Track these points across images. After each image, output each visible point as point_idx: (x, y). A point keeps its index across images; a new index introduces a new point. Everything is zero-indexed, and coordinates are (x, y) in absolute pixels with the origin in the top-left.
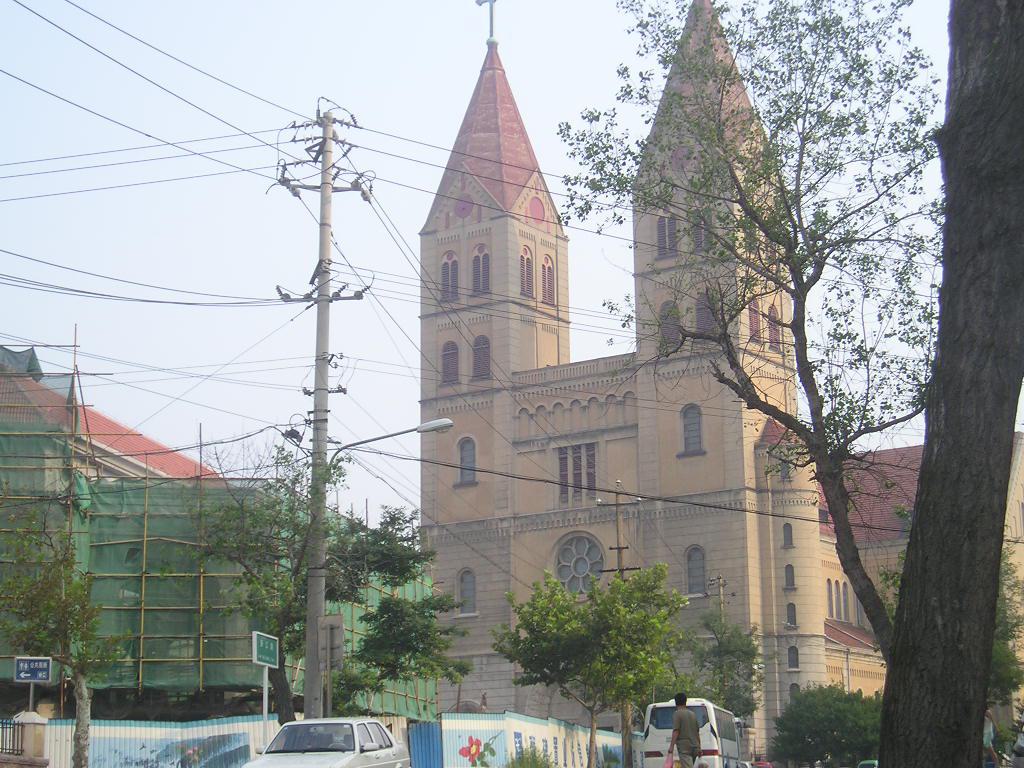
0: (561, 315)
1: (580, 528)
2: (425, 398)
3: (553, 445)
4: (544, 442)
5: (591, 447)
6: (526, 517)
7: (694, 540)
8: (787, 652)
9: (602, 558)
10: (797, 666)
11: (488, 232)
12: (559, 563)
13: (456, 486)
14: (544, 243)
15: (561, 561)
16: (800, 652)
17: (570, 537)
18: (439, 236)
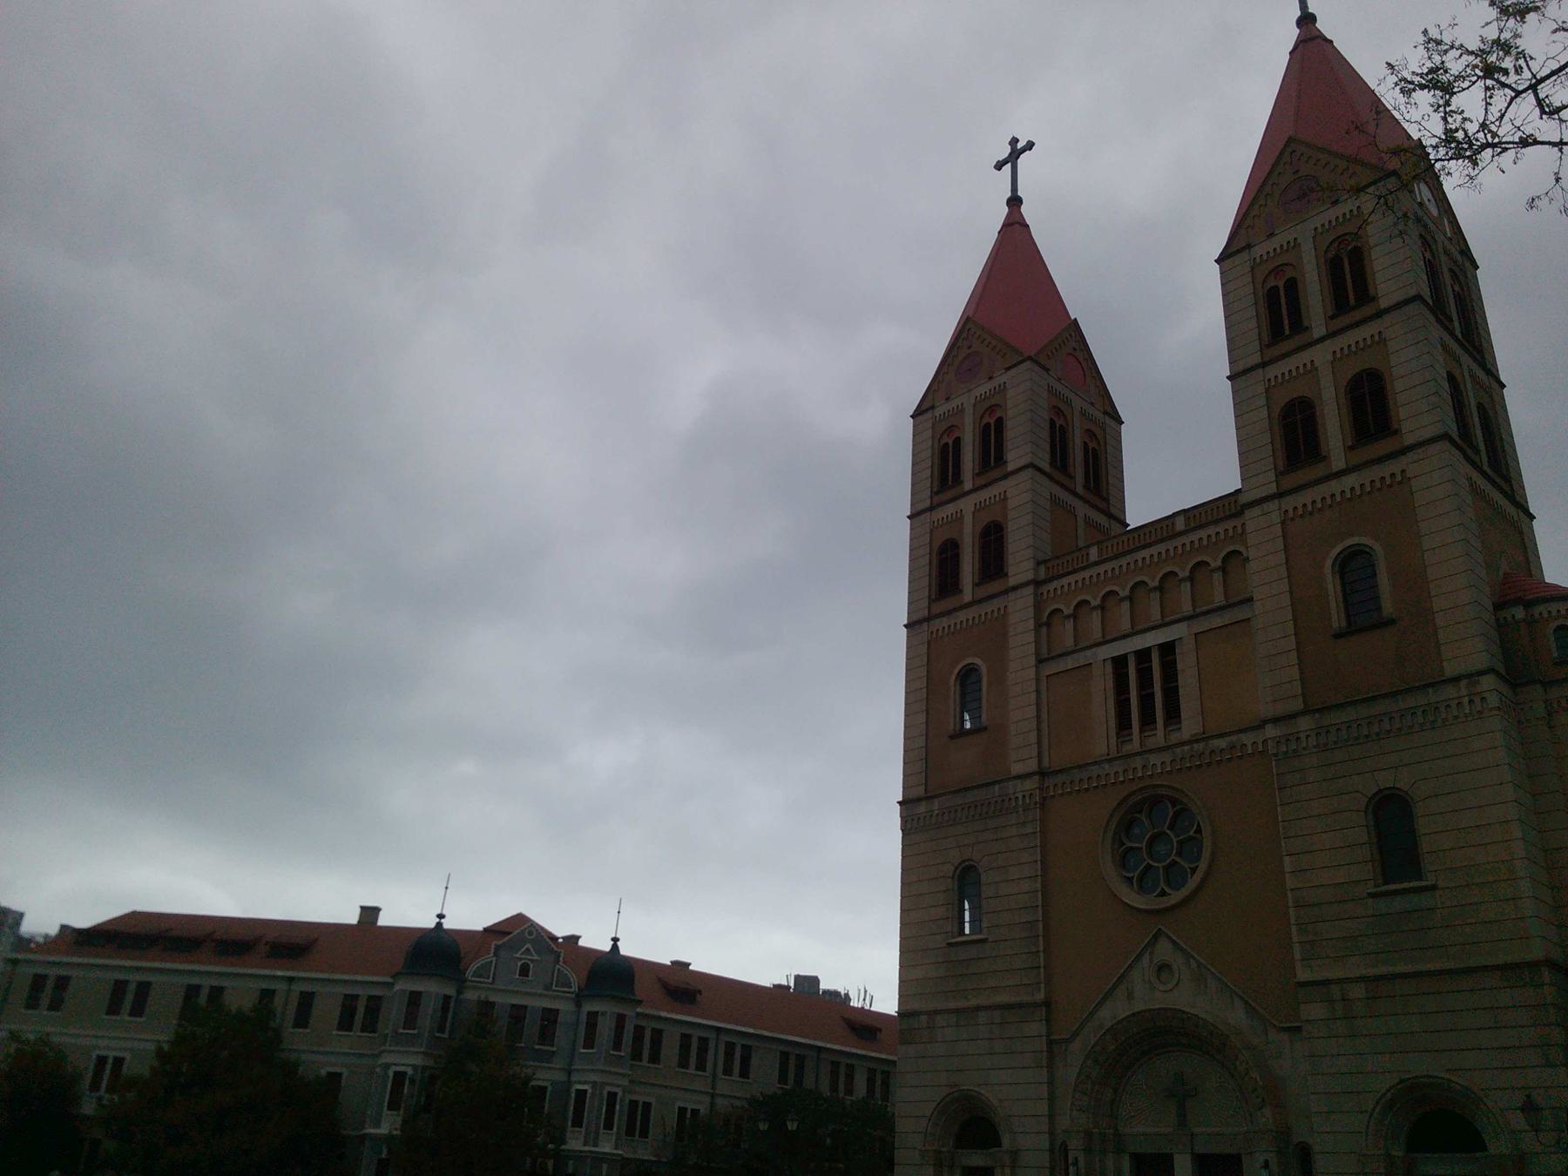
0: (1113, 510)
2: (915, 618)
7: (1385, 780)
11: (1002, 389)
13: (952, 737)
14: (1083, 413)
18: (938, 412)
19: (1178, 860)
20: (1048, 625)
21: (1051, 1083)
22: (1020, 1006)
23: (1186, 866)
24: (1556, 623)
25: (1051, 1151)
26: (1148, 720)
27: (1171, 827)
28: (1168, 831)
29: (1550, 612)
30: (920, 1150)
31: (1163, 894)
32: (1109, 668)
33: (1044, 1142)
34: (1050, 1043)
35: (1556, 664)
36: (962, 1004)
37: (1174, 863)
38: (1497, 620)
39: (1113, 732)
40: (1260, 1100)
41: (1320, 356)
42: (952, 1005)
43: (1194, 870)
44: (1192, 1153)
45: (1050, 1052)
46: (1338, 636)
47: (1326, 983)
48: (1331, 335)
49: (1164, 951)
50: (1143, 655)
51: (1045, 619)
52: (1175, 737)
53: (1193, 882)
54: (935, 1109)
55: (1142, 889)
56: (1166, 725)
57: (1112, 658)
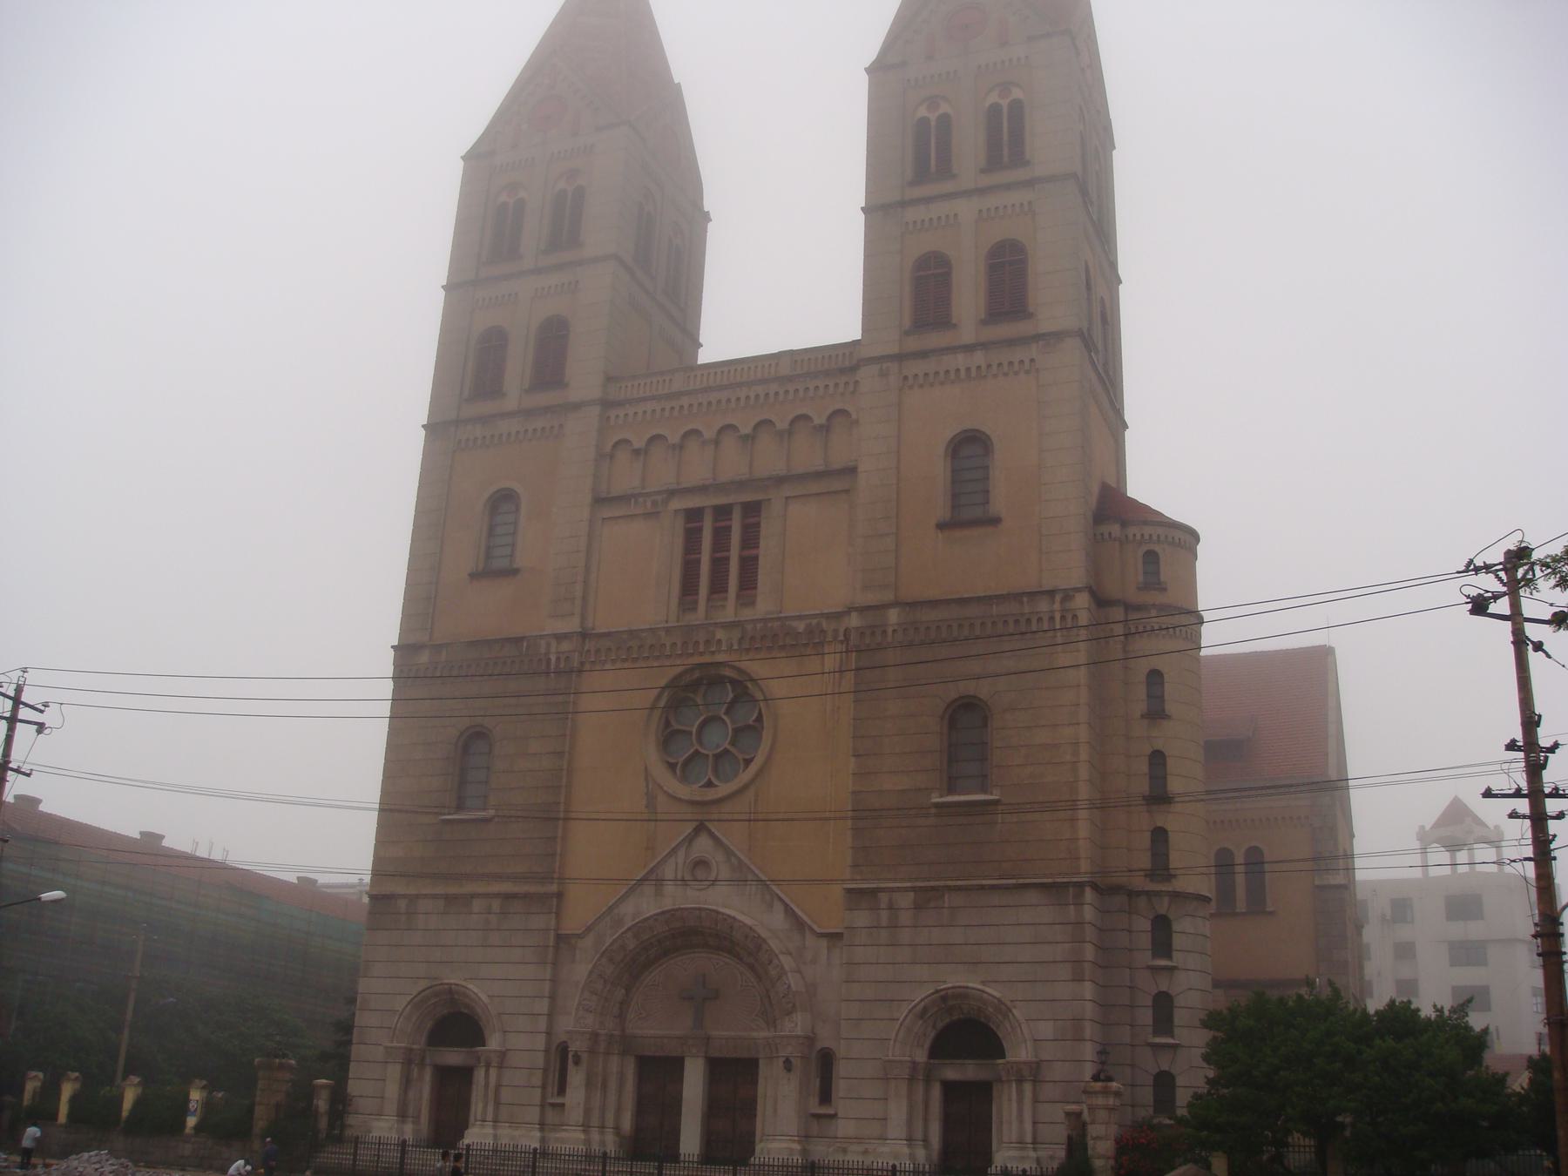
1: (720, 658)
3: (678, 504)
4: (659, 498)
5: (752, 510)
6: (608, 634)
7: (968, 688)
8: (1147, 925)
9: (759, 719)
10: (1170, 957)
12: (668, 723)
15: (673, 722)
16: (1176, 927)
17: (697, 674)
19: (732, 749)
20: (612, 457)
21: (554, 981)
22: (526, 896)
23: (740, 757)
24: (1145, 548)
25: (547, 1051)
26: (718, 587)
27: (727, 713)
28: (725, 717)
29: (1142, 535)
30: (386, 1048)
31: (709, 784)
32: (680, 524)
33: (540, 1041)
34: (559, 937)
35: (1139, 589)
36: (453, 890)
37: (726, 751)
38: (1095, 535)
39: (674, 601)
40: (791, 1005)
41: (966, 209)
42: (440, 890)
43: (748, 762)
44: (706, 1057)
45: (557, 948)
46: (941, 526)
47: (874, 892)
48: (981, 191)
49: (703, 845)
50: (723, 512)
51: (608, 448)
52: (747, 614)
53: (746, 776)
54: (409, 1003)
55: (684, 779)
56: (738, 597)
57: (685, 510)
